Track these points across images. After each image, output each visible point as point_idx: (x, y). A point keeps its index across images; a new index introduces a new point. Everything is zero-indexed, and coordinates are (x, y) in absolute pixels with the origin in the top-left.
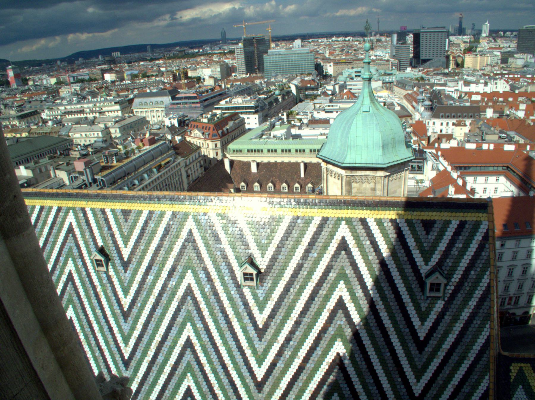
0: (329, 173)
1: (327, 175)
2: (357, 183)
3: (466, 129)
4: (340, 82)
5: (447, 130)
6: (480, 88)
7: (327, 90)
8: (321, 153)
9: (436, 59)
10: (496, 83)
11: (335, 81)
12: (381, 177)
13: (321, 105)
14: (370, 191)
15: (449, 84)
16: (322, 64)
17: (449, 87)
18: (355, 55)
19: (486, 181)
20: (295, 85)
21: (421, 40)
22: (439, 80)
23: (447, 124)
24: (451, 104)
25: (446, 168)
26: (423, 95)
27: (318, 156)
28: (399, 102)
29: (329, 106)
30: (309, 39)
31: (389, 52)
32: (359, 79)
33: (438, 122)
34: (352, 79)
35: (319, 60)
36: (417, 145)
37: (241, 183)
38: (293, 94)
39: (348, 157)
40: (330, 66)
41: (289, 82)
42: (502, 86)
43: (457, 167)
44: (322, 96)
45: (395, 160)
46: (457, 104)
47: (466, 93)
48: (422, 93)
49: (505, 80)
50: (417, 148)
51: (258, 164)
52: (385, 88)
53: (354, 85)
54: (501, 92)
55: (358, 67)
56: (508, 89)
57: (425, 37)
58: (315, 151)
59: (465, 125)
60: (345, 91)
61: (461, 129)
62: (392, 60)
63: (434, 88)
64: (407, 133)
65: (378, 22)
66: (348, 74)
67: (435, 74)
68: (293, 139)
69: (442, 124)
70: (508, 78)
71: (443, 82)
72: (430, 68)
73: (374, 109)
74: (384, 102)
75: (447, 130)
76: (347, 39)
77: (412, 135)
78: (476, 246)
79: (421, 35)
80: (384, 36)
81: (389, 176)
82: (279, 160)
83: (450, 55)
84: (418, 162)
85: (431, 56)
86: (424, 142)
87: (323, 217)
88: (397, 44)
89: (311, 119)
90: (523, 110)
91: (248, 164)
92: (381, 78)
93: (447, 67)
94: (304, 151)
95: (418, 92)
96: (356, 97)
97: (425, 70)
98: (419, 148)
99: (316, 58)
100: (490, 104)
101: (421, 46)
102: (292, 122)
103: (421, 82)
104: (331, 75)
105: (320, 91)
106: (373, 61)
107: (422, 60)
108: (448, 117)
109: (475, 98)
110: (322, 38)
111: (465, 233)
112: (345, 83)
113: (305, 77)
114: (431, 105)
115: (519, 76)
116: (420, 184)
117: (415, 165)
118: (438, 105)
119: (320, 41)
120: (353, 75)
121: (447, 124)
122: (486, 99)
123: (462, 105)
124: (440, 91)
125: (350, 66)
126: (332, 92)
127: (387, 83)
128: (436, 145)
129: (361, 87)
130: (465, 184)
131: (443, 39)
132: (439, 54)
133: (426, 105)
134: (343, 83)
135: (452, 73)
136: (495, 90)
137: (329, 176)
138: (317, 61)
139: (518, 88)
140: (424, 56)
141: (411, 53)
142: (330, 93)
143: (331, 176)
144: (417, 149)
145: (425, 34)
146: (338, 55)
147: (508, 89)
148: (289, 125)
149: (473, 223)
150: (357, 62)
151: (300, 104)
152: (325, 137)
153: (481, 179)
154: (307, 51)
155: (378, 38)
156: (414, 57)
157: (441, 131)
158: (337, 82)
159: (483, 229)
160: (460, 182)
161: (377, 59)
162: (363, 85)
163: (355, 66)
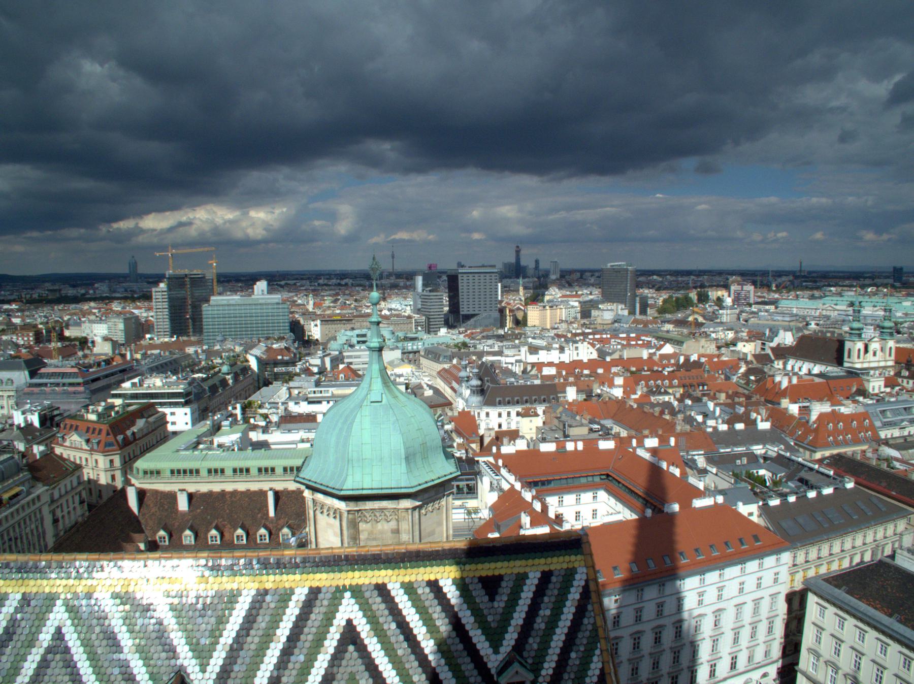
0: (319, 509)
1: (315, 511)
2: (367, 522)
3: (538, 421)
4: (332, 352)
5: (509, 423)
6: (554, 356)
7: (310, 365)
8: (301, 475)
9: (484, 315)
10: (577, 348)
11: (324, 350)
12: (407, 509)
13: (300, 390)
14: (390, 534)
15: (506, 352)
16: (302, 322)
17: (507, 356)
18: (356, 308)
19: (578, 500)
20: (257, 358)
21: (460, 285)
22: (491, 346)
23: (509, 414)
24: (512, 383)
25: (513, 486)
26: (468, 369)
27: (298, 479)
28: (430, 383)
29: (315, 392)
30: (280, 281)
31: (411, 303)
32: (363, 347)
33: (494, 412)
34: (352, 346)
35: (297, 316)
36: (464, 451)
37: (159, 531)
38: (253, 371)
39: (350, 478)
40: (316, 325)
41: (246, 352)
42: (585, 352)
43: (530, 483)
44: (303, 376)
46: (522, 382)
47: (533, 365)
48: (466, 368)
49: (589, 343)
50: (464, 457)
51: (191, 496)
52: (406, 361)
53: (356, 357)
54: (585, 361)
55: (361, 328)
56: (595, 355)
57: (465, 281)
58: (292, 469)
59: (536, 415)
60: (341, 366)
61: (531, 421)
62: (417, 316)
63: (484, 359)
64: (446, 432)
65: (393, 257)
66: (345, 338)
67: (483, 337)
68: (253, 450)
69: (500, 415)
70: (594, 339)
71: (496, 349)
72: (475, 328)
73: (390, 397)
74: (406, 384)
75: (509, 423)
76: (343, 282)
77: (454, 435)
78: (573, 610)
79: (460, 278)
80: (401, 278)
81: (420, 507)
82: (229, 487)
83: (505, 307)
84: (467, 480)
85: (477, 309)
86: (474, 446)
87: (311, 588)
88: (423, 290)
89: (283, 414)
90: (620, 386)
91: (171, 498)
92: (400, 345)
93: (502, 325)
94: (273, 470)
95: (460, 366)
96: (359, 376)
97: (469, 332)
98: (467, 456)
99: (292, 313)
100: (571, 379)
101: (460, 294)
102: (252, 421)
103: (462, 350)
104: (317, 340)
105: (299, 366)
106: (386, 317)
107: (463, 315)
108: (509, 403)
109: (547, 371)
110: (302, 279)
111: (553, 591)
112: (341, 353)
113: (273, 344)
114: (481, 386)
115: (609, 336)
116: (473, 516)
117: (462, 484)
118: (491, 385)
119: (298, 284)
120: (354, 340)
121: (509, 414)
122: (564, 373)
123: (529, 383)
124: (493, 364)
125: (349, 326)
126: (319, 368)
127: (410, 353)
128: (494, 449)
129: (368, 360)
130: (545, 508)
131: (493, 284)
132: (488, 306)
133: (473, 386)
134: (337, 353)
135: (510, 335)
136: (576, 358)
137: (318, 512)
138: (294, 317)
139: (610, 354)
141: (445, 306)
142: (315, 370)
143: (322, 513)
144: (464, 458)
145: (465, 275)
146: (329, 307)
147: (595, 355)
148: (245, 425)
149: (563, 573)
150: (361, 319)
151: (264, 389)
152: (308, 445)
153: (569, 498)
154: (277, 301)
155: (392, 281)
156: (450, 311)
157: (500, 426)
158: (328, 352)
159: (579, 581)
160: (537, 506)
161: (391, 315)
162: (371, 357)
163: (357, 325)
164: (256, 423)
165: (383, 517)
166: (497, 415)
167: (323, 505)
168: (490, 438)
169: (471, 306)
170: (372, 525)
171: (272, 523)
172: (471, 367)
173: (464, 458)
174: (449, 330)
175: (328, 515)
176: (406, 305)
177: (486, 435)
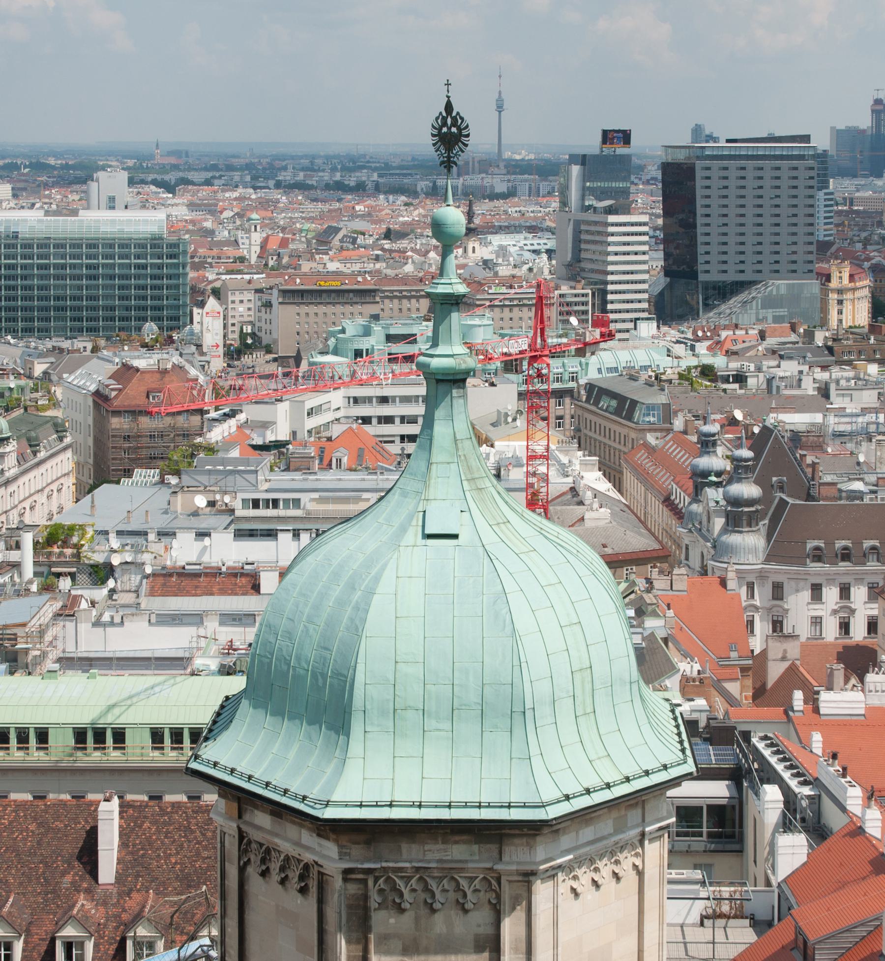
0: (255, 858)
1: (242, 870)
2: (400, 910)
24: (859, 495)
45: (592, 781)
48: (714, 444)
65: (500, 108)
79: (699, 174)
85: (748, 268)
107: (707, 286)
118: (790, 501)
137: (252, 872)
140: (714, 267)
143: (264, 874)
144: (702, 724)
164: (73, 592)
165: (452, 895)
166: (806, 595)
167: (268, 851)
168: (786, 665)
169: (733, 258)
170: (417, 919)
171: (105, 904)
172: (729, 441)
173: (702, 724)
174: (665, 329)
175: (283, 882)
176: (536, 252)
177: (771, 655)
